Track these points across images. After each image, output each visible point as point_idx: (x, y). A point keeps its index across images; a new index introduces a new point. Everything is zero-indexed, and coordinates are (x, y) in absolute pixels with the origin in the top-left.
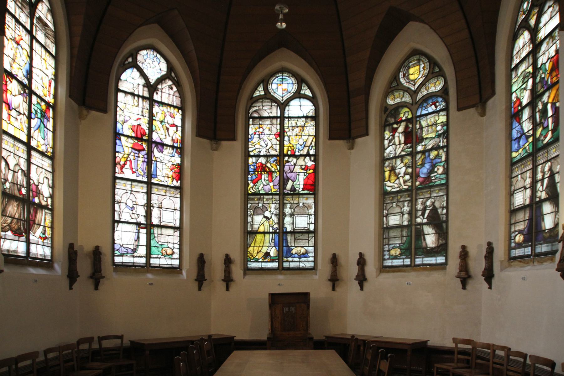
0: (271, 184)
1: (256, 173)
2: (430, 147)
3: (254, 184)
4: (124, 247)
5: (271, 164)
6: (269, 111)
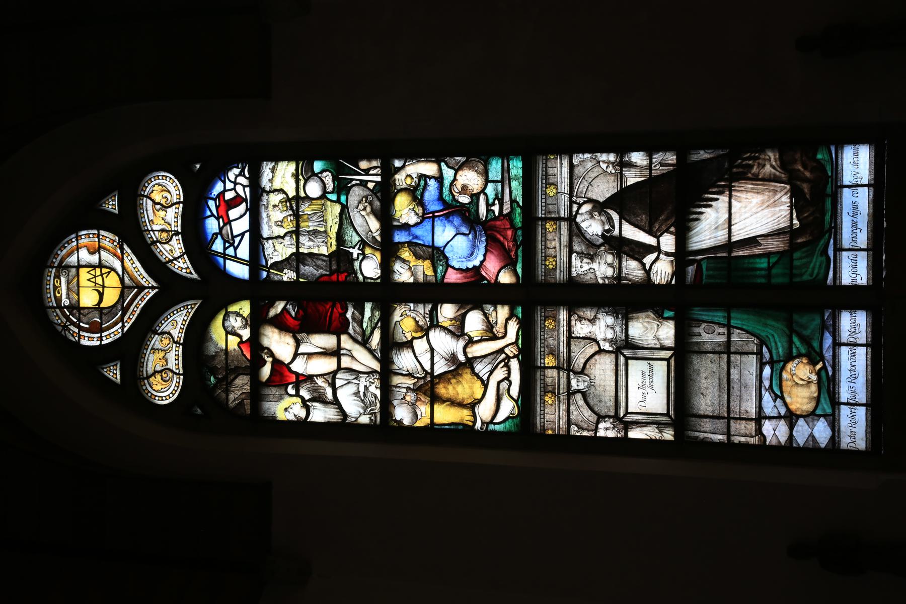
2: (374, 225)
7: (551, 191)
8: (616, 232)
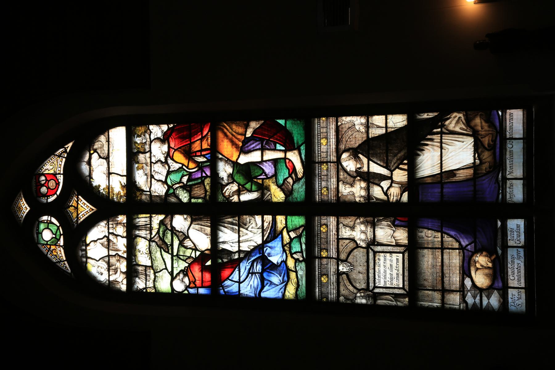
8: (365, 169)
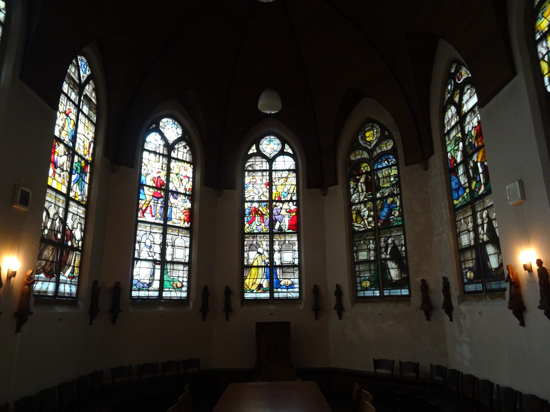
0: (263, 225)
1: (251, 215)
2: (386, 194)
3: (250, 225)
4: (141, 282)
5: (262, 208)
6: (260, 165)
7: (396, 231)
